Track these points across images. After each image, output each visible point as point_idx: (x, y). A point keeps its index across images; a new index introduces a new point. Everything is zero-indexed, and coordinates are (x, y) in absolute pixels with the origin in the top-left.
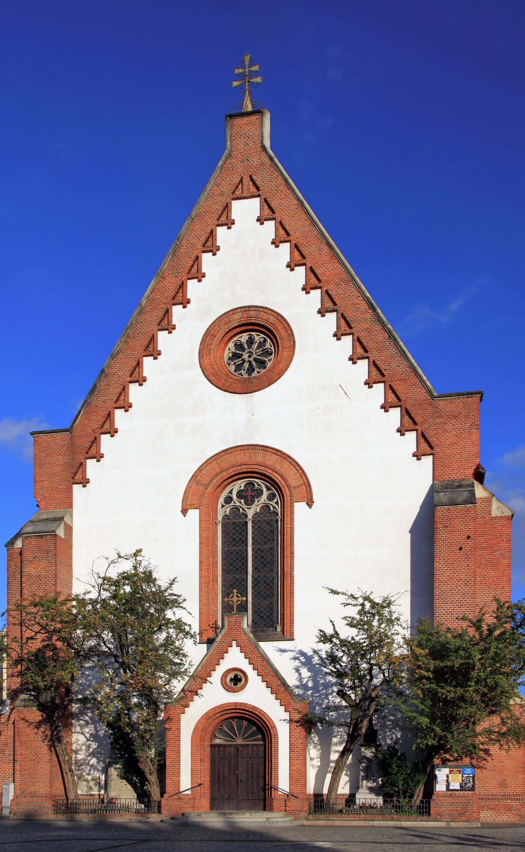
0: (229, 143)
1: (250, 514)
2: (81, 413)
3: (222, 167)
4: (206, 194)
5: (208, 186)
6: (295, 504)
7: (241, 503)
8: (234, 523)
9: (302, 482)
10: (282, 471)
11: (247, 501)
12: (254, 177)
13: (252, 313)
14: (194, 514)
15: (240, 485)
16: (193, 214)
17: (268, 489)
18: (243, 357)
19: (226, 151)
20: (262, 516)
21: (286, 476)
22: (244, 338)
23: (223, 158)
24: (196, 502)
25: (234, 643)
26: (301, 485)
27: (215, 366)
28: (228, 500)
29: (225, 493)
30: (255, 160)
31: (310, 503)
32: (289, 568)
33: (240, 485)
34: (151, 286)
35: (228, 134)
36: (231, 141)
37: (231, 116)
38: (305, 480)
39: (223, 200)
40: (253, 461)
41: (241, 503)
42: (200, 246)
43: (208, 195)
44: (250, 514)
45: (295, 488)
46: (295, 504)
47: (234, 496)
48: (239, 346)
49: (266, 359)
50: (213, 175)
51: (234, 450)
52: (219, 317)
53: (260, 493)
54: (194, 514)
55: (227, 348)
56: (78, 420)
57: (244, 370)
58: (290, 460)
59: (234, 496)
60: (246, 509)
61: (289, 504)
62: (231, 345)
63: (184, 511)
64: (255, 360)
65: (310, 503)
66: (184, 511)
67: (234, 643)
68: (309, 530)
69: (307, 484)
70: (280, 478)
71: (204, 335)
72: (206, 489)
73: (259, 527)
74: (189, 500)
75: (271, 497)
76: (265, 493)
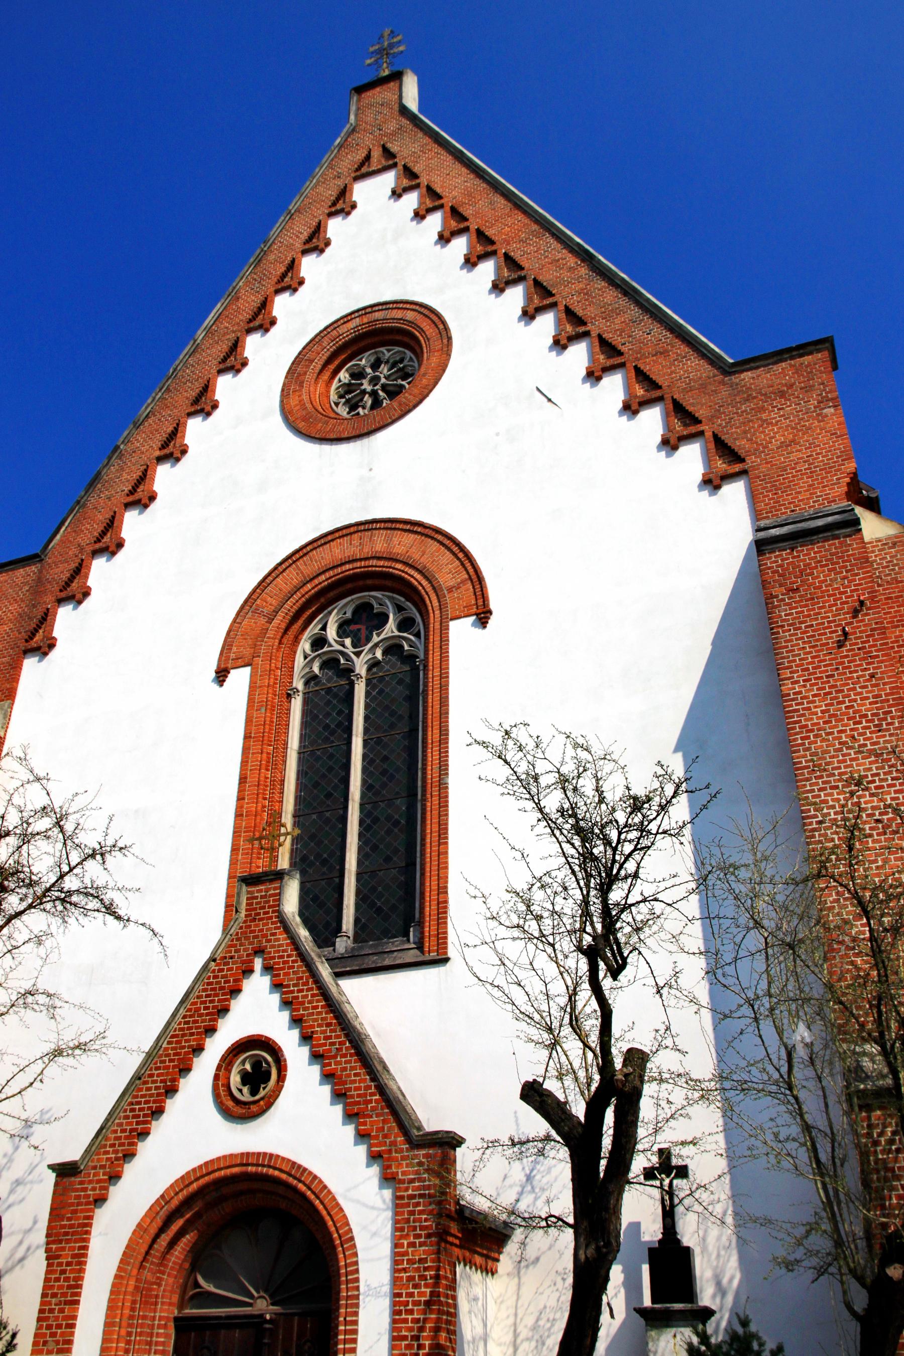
0: (352, 117)
1: (361, 666)
2: (66, 524)
3: (341, 146)
4: (314, 181)
5: (317, 170)
6: (454, 625)
7: (343, 646)
8: (329, 690)
9: (466, 576)
10: (424, 561)
11: (359, 640)
12: (389, 145)
13: (377, 315)
14: (240, 678)
16: (292, 207)
17: (399, 609)
18: (363, 387)
19: (348, 126)
20: (387, 667)
21: (432, 568)
23: (342, 135)
24: (247, 652)
25: (258, 963)
26: (463, 582)
27: (309, 406)
28: (319, 642)
29: (313, 629)
30: (392, 126)
31: (483, 617)
32: (436, 768)
34: (212, 315)
35: (353, 108)
36: (356, 115)
37: (360, 90)
38: (471, 571)
39: (340, 183)
40: (367, 551)
41: (343, 646)
42: (299, 246)
43: (318, 181)
44: (361, 666)
45: (450, 590)
46: (454, 625)
47: (331, 633)
48: (358, 375)
49: (404, 383)
50: (327, 156)
51: (330, 538)
52: (321, 332)
54: (240, 678)
55: (337, 379)
56: (58, 537)
57: (364, 408)
58: (440, 537)
59: (331, 633)
60: (352, 656)
61: (437, 625)
63: (221, 676)
64: (384, 388)
65: (483, 617)
66: (221, 676)
67: (258, 963)
68: (484, 680)
69: (474, 577)
70: (418, 577)
71: (293, 363)
72: (270, 621)
73: (381, 692)
74: (234, 649)
75: (405, 624)
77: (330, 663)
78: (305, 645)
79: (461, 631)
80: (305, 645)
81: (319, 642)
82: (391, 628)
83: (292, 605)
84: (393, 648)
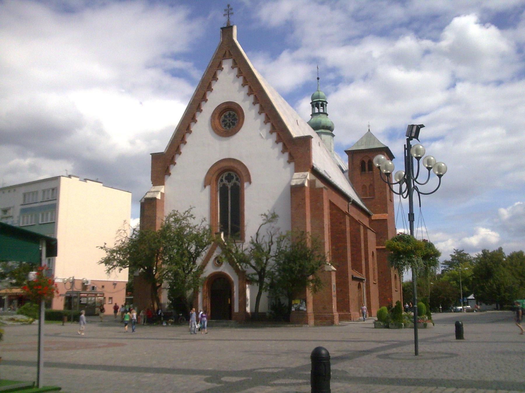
1: (229, 187)
14: (208, 188)
15: (226, 174)
22: (227, 113)
28: (222, 181)
29: (220, 178)
33: (226, 174)
44: (229, 187)
47: (224, 179)
48: (225, 117)
53: (233, 177)
54: (208, 188)
59: (224, 179)
62: (223, 116)
66: (205, 186)
75: (237, 179)
76: (235, 178)
77: (224, 185)
78: (219, 180)
79: (246, 184)
80: (219, 180)
81: (222, 181)
82: (234, 181)
83: (217, 174)
84: (235, 184)
